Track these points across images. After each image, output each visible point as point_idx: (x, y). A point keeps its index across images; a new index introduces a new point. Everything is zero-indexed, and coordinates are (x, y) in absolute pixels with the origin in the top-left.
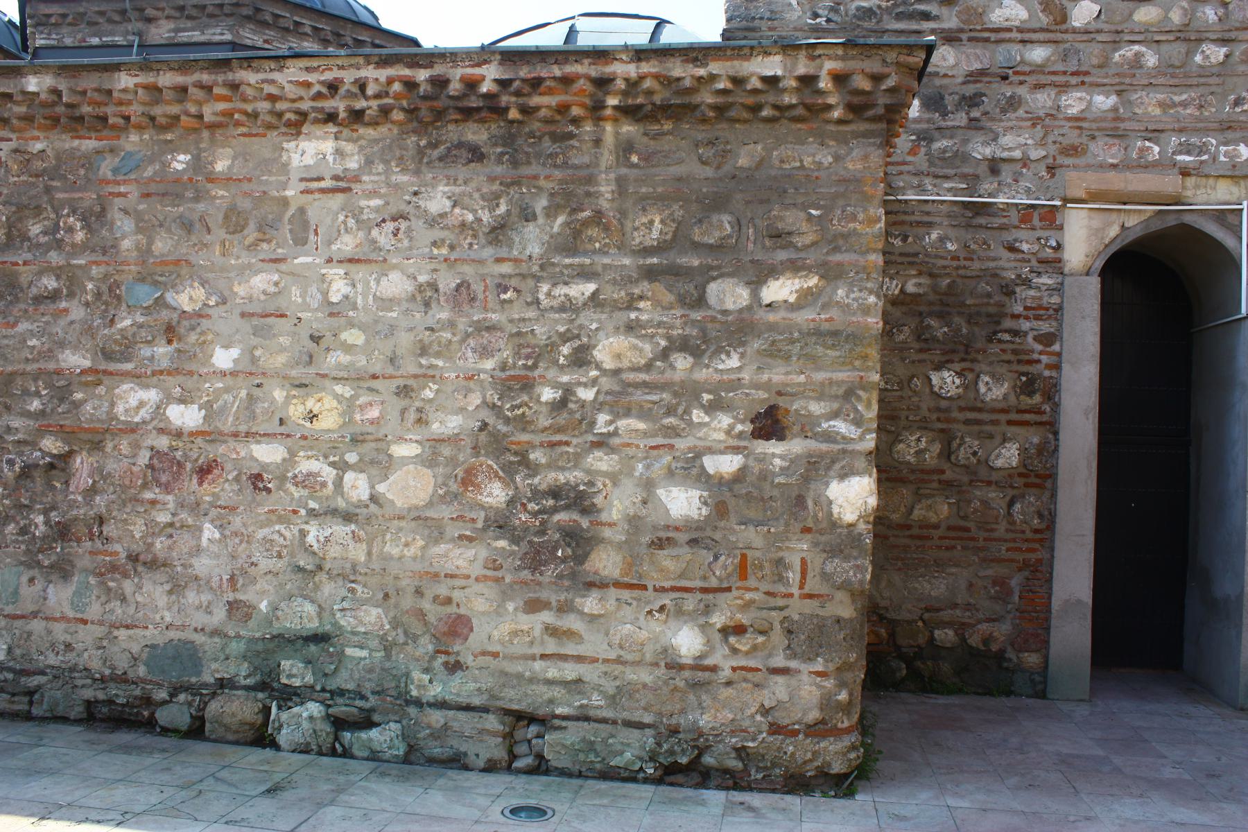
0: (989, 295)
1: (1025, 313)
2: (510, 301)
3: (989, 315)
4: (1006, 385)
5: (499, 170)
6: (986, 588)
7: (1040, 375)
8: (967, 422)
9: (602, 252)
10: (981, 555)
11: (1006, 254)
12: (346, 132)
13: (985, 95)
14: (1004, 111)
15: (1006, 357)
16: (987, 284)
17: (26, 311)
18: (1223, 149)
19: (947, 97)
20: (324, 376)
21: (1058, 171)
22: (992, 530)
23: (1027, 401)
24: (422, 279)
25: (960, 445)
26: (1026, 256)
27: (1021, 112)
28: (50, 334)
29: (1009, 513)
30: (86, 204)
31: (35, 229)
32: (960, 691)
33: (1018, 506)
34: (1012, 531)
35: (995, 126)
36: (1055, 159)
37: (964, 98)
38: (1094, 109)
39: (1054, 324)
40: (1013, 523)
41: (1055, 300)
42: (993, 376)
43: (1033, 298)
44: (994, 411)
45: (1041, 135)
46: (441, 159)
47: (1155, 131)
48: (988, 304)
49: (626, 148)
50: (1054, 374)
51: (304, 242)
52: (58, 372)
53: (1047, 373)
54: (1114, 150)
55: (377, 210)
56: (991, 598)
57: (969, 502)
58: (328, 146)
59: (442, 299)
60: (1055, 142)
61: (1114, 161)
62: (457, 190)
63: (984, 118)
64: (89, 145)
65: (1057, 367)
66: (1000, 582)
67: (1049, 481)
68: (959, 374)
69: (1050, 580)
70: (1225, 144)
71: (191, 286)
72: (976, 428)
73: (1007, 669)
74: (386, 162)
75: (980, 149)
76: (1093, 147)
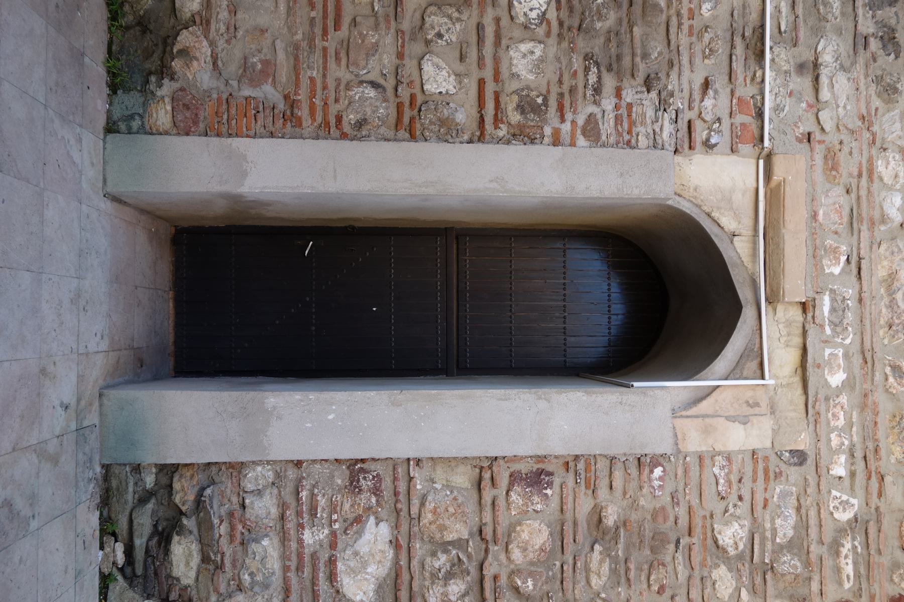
0: (645, 56)
1: (623, 104)
3: (619, 58)
4: (531, 77)
6: (260, 51)
7: (545, 121)
8: (480, 27)
10: (304, 44)
11: (698, 81)
13: (897, 57)
14: (879, 80)
15: (566, 78)
16: (660, 54)
18: (840, 352)
19: (894, 10)
21: (806, 145)
22: (338, 59)
23: (510, 105)
25: (450, 17)
26: (696, 104)
27: (876, 102)
29: (361, 82)
32: (114, 17)
33: (371, 93)
34: (338, 85)
35: (860, 67)
36: (819, 142)
37: (893, 30)
38: (883, 194)
39: (612, 140)
40: (348, 87)
41: (643, 141)
42: (542, 60)
43: (644, 115)
44: (496, 60)
45: (850, 126)
47: (859, 269)
48: (633, 55)
50: (546, 140)
53: (548, 131)
54: (835, 217)
56: (245, 58)
57: (376, 27)
60: (841, 143)
61: (820, 217)
63: (869, 55)
65: (556, 141)
66: (268, 70)
67: (407, 135)
68: (543, 17)
69: (272, 135)
70: (846, 356)
72: (474, 39)
73: (147, 82)
75: (830, 49)
76: (838, 192)
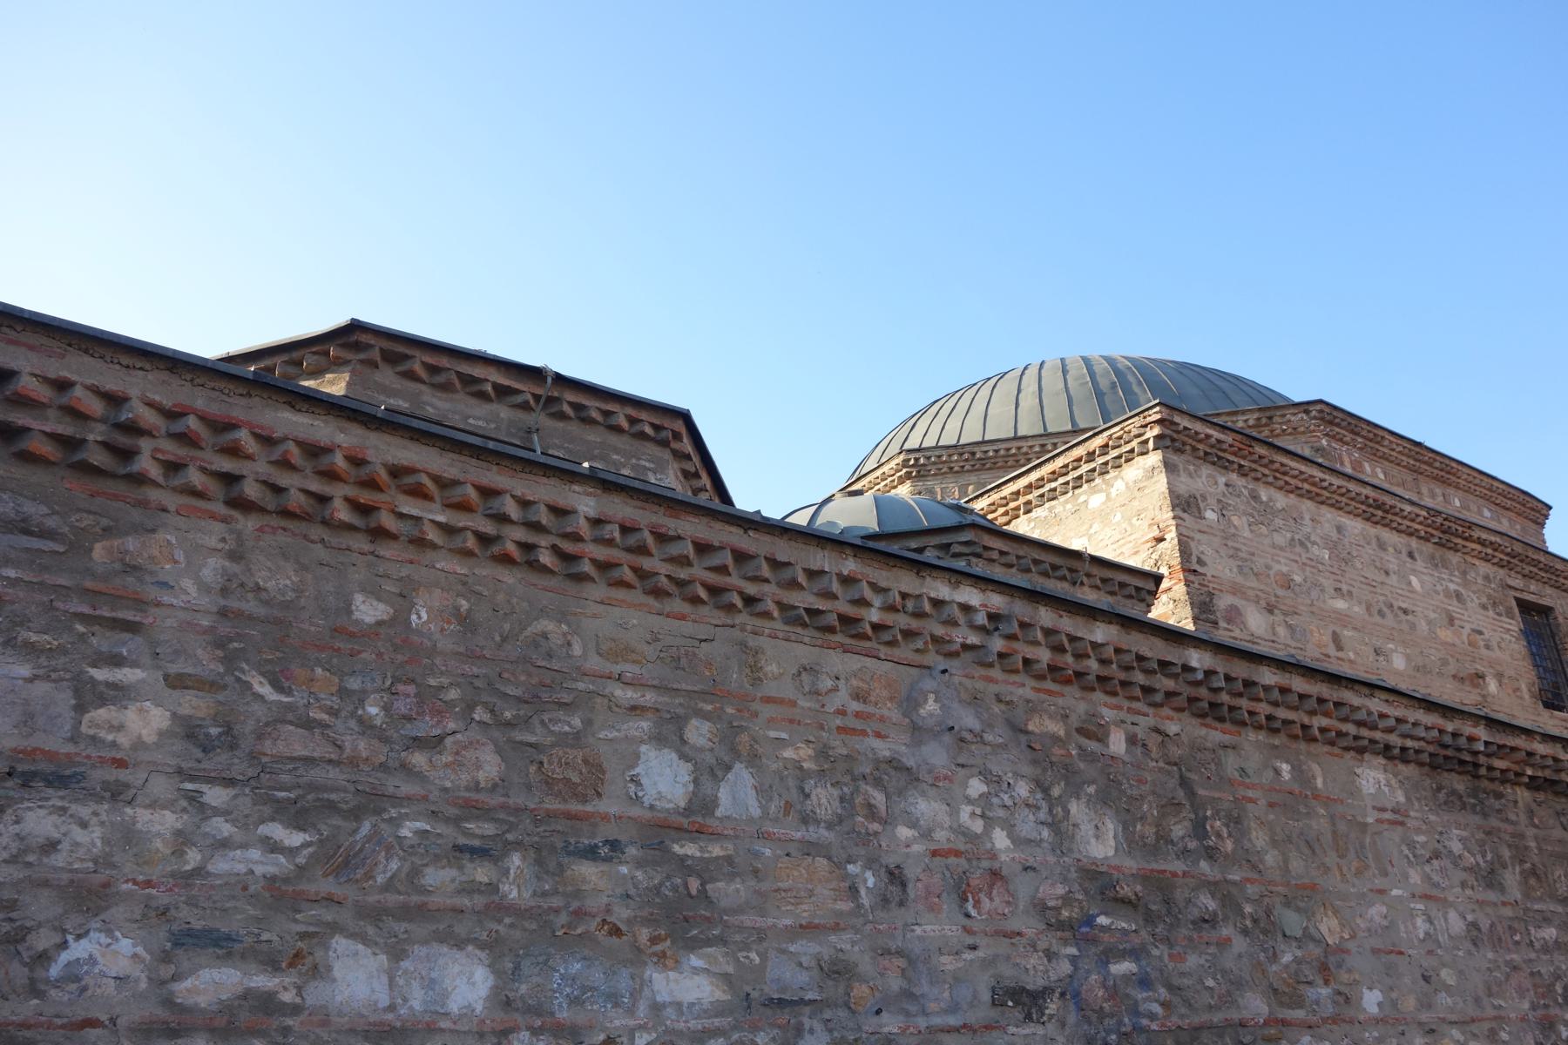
2: (1517, 943)
5: (1477, 819)
9: (1541, 899)
12: (1390, 766)
17: (1190, 939)
20: (1443, 1020)
24: (1470, 918)
28: (1224, 972)
30: (1226, 805)
31: (1178, 831)
46: (1446, 803)
49: (1531, 813)
51: (1385, 874)
52: (1242, 1025)
55: (1424, 845)
58: (1381, 777)
59: (1485, 938)
62: (1464, 834)
64: (1215, 735)
71: (1326, 915)
74: (1418, 799)
